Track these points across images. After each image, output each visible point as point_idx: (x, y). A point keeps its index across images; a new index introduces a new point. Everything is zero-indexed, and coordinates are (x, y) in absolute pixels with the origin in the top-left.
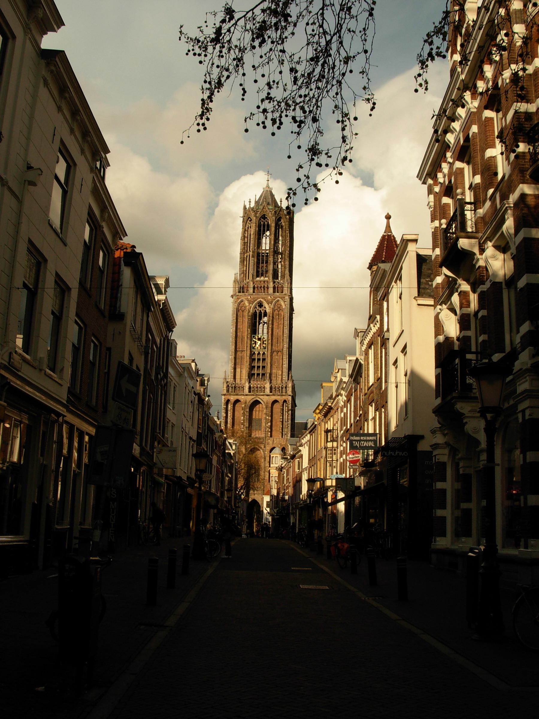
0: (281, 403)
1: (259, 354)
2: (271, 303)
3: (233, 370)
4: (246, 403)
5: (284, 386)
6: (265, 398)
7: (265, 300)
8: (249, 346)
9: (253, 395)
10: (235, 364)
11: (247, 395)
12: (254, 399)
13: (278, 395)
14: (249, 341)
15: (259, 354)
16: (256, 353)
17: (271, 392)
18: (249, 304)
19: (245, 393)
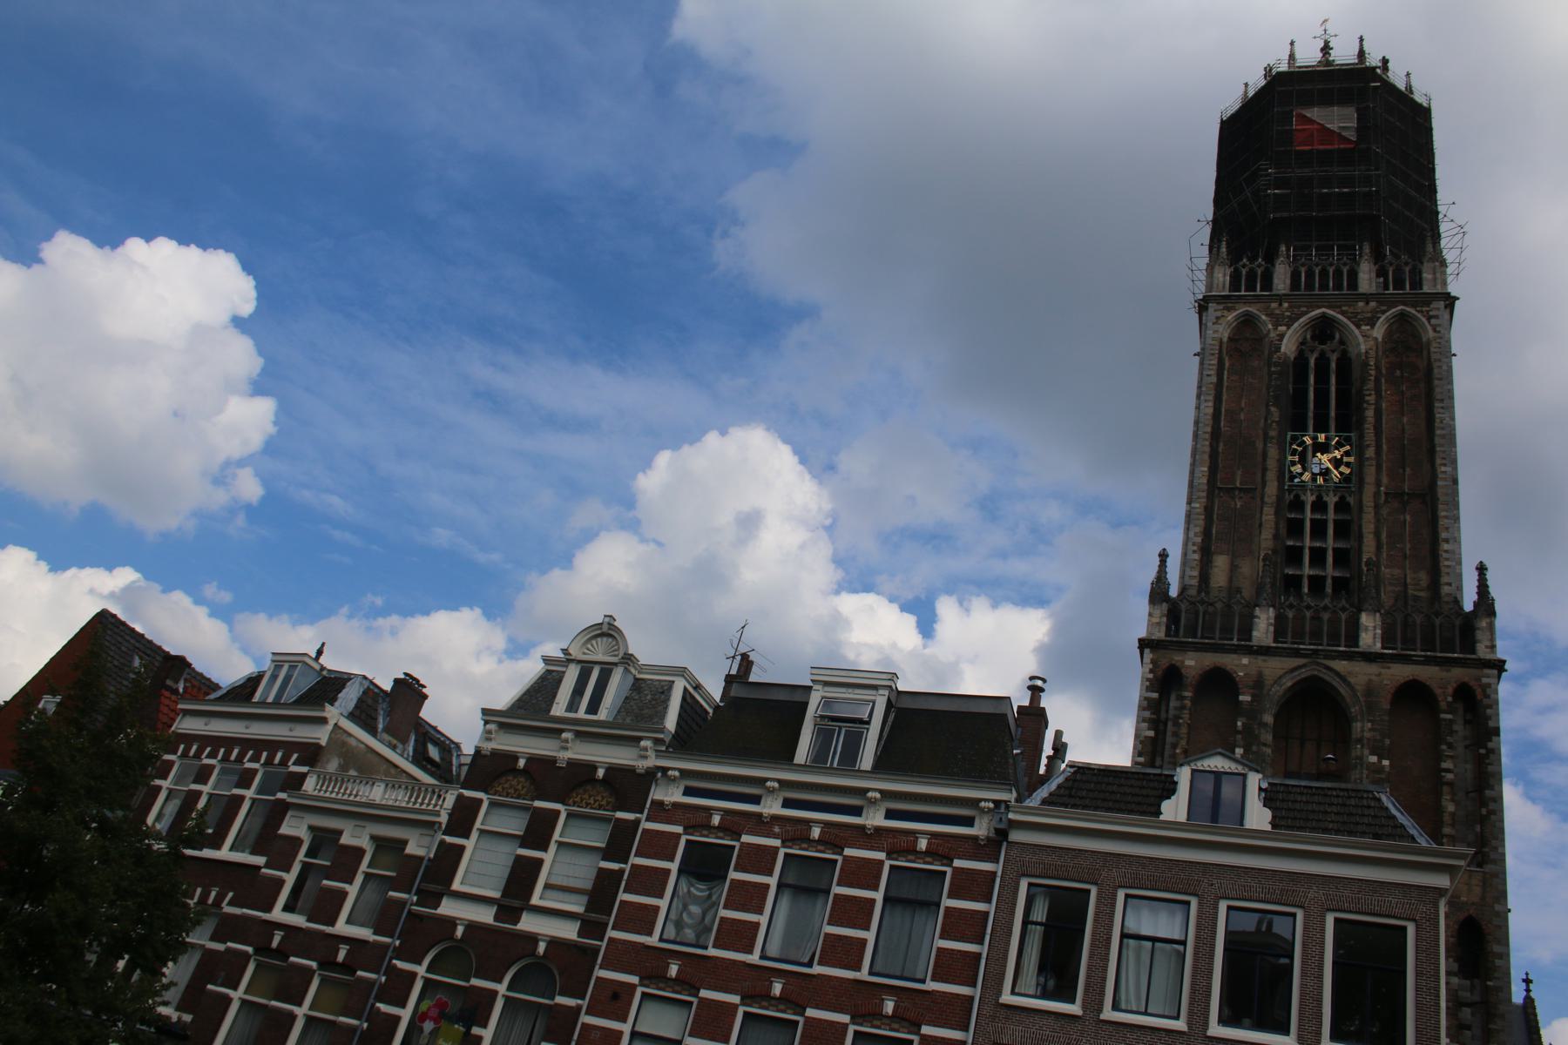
0: (1445, 697)
1: (1319, 506)
2: (1372, 322)
3: (1196, 556)
4: (1258, 684)
5: (1458, 622)
6: (1360, 673)
7: (1343, 313)
8: (1272, 464)
9: (1296, 653)
10: (1207, 533)
11: (1264, 651)
12: (1304, 673)
13: (1428, 661)
14: (1273, 452)
15: (1319, 506)
16: (1309, 499)
17: (1387, 639)
18: (1276, 326)
19: (1255, 642)
